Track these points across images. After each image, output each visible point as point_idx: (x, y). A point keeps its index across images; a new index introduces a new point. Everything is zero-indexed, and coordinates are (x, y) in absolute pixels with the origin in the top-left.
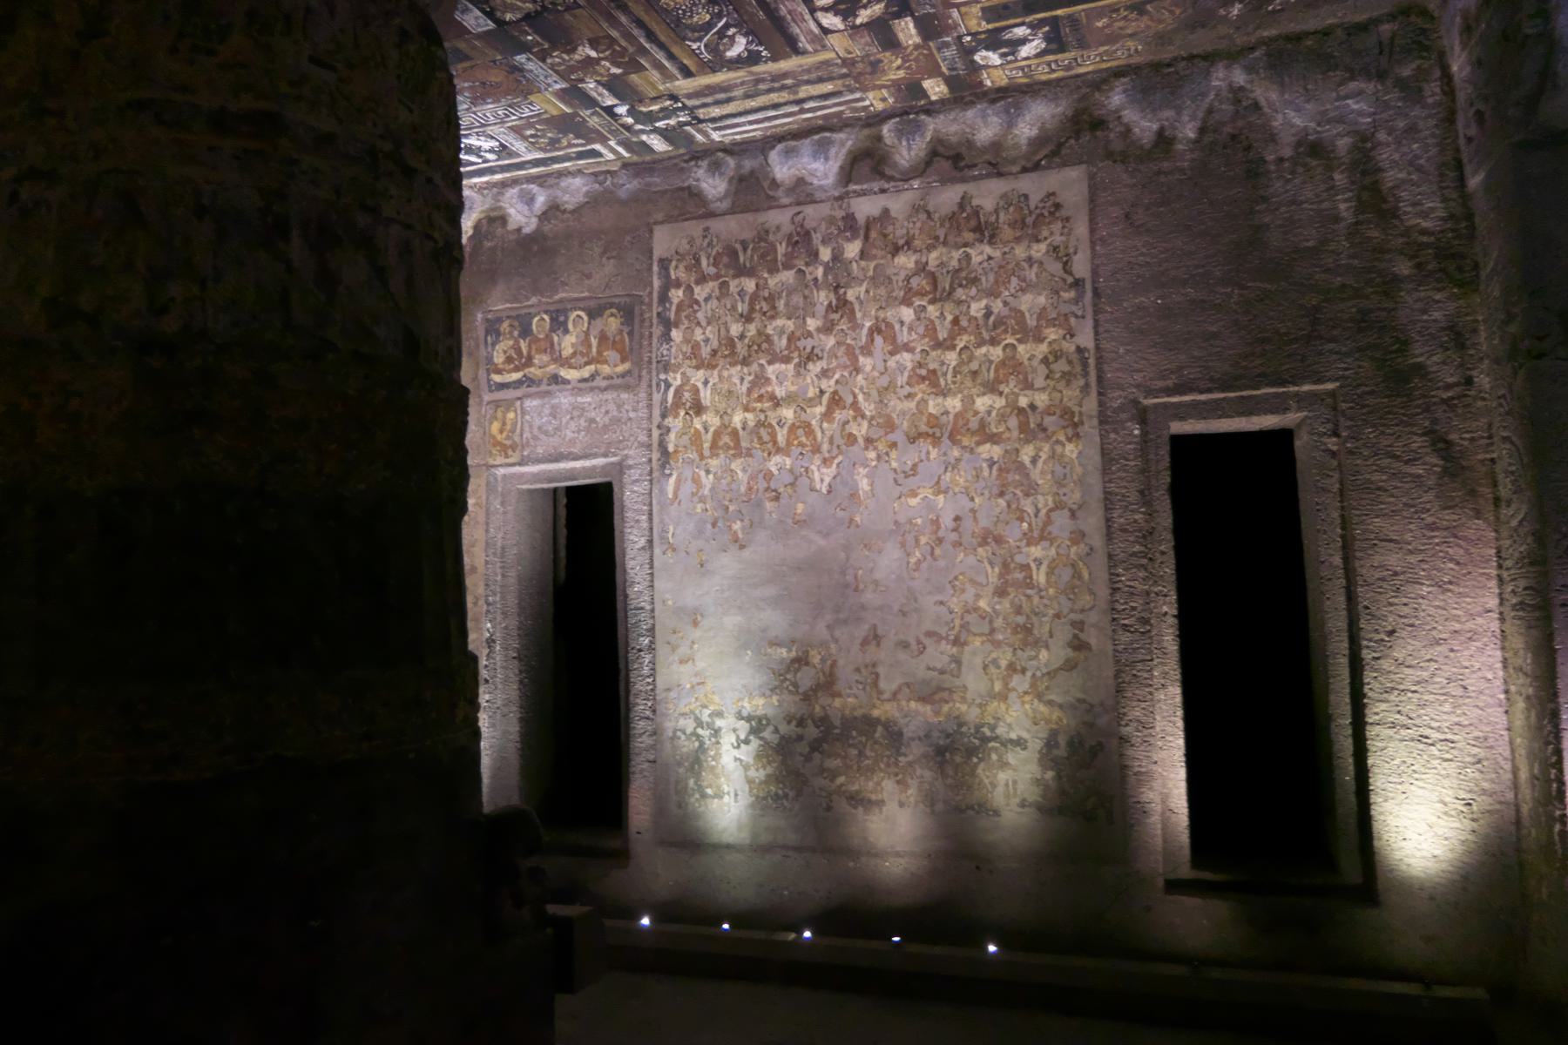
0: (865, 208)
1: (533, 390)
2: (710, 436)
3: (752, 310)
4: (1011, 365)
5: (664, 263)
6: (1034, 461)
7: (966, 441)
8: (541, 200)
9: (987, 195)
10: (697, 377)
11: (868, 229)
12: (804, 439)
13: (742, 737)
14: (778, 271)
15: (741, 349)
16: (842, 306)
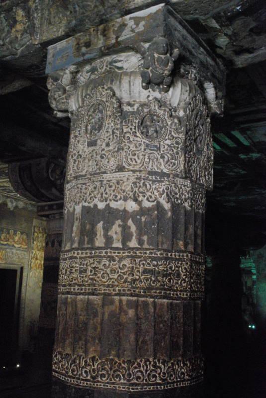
8: (14, 204)
10: (38, 252)
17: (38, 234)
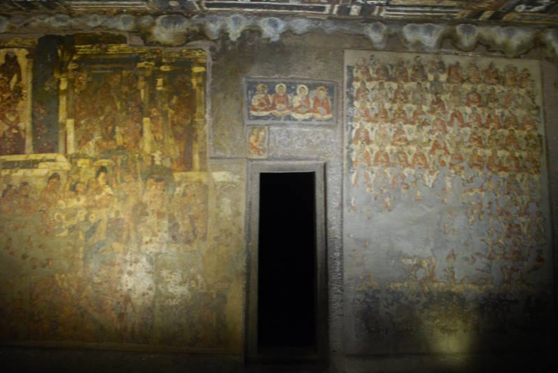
0: (449, 60)
1: (276, 122)
2: (374, 155)
3: (396, 98)
4: (511, 138)
5: (350, 69)
6: (522, 180)
7: (494, 169)
8: (282, 26)
9: (501, 64)
10: (368, 126)
11: (450, 70)
12: (421, 161)
13: (390, 302)
14: (408, 81)
15: (390, 116)
16: (438, 102)
17: (363, 83)
